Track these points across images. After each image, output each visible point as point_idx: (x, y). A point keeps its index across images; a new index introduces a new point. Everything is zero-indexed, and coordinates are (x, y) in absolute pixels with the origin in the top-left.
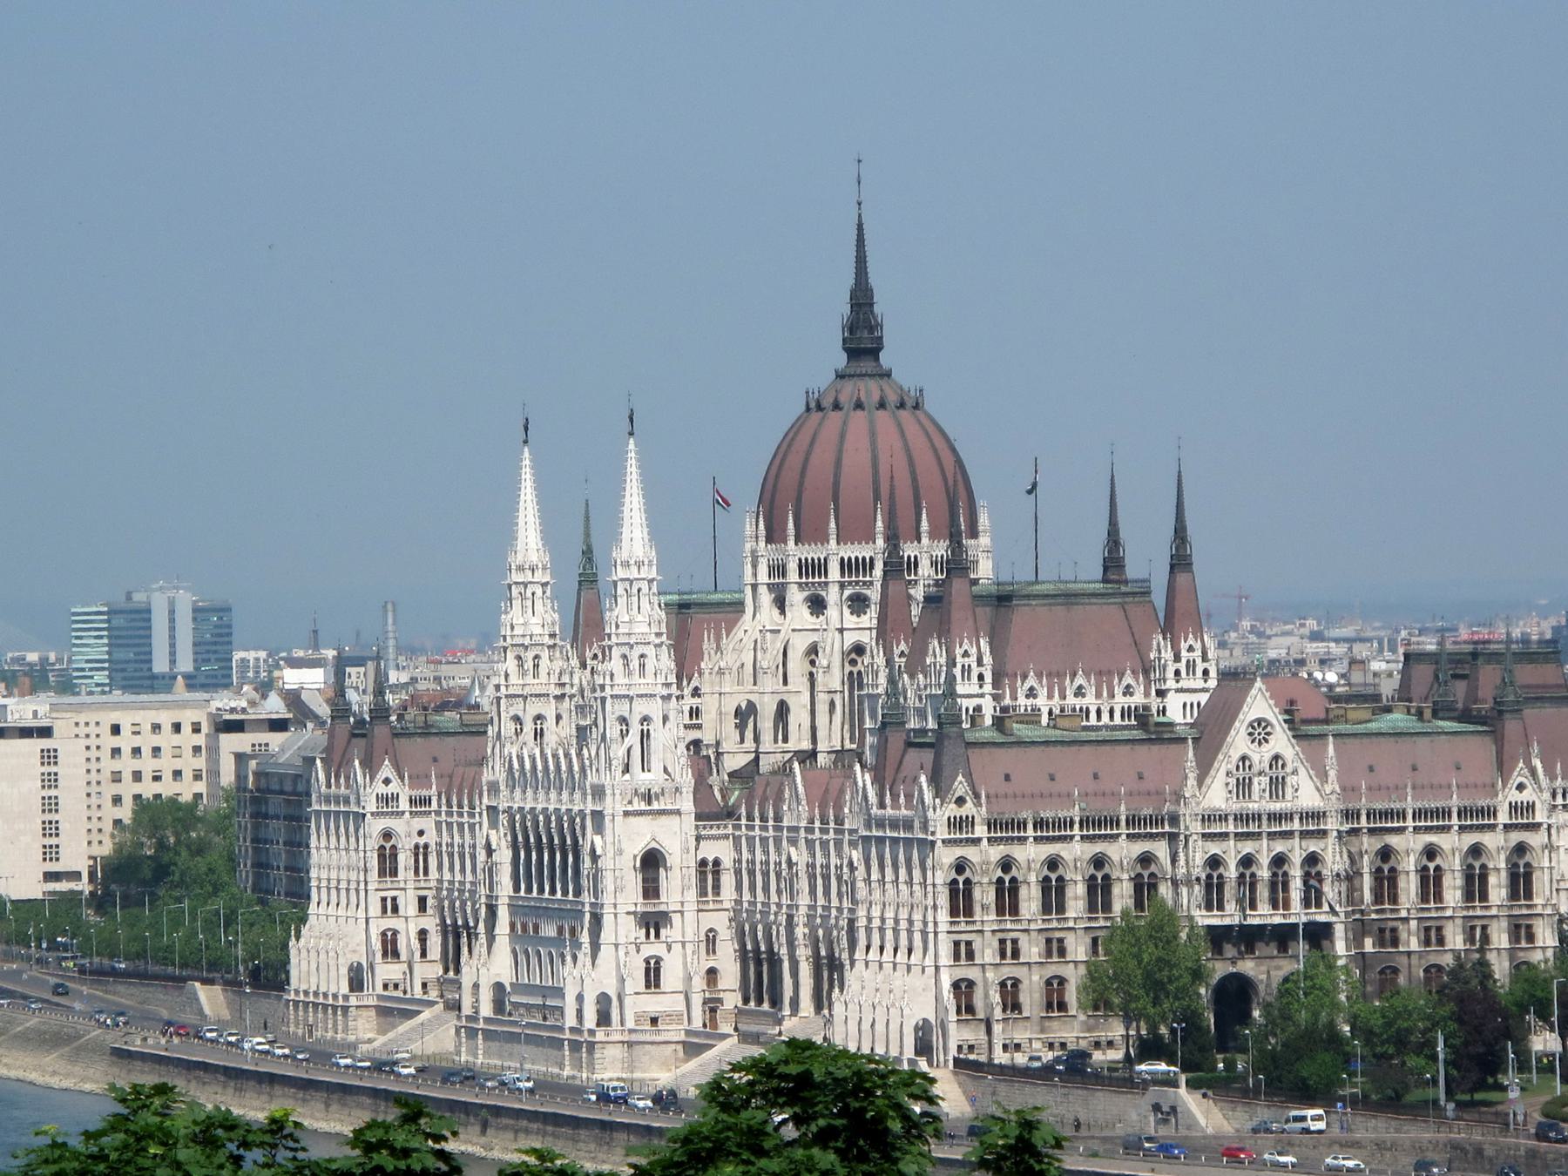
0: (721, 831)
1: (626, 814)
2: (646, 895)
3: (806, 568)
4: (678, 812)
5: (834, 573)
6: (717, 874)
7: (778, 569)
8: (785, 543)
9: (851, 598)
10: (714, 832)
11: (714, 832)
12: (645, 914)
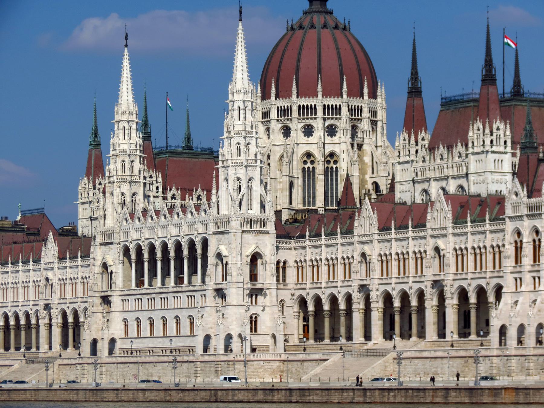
0: (287, 245)
1: (243, 232)
2: (251, 280)
3: (304, 110)
4: (267, 232)
5: (320, 112)
6: (284, 268)
7: (285, 112)
8: (290, 96)
9: (328, 127)
10: (284, 245)
11: (284, 245)
12: (252, 289)
